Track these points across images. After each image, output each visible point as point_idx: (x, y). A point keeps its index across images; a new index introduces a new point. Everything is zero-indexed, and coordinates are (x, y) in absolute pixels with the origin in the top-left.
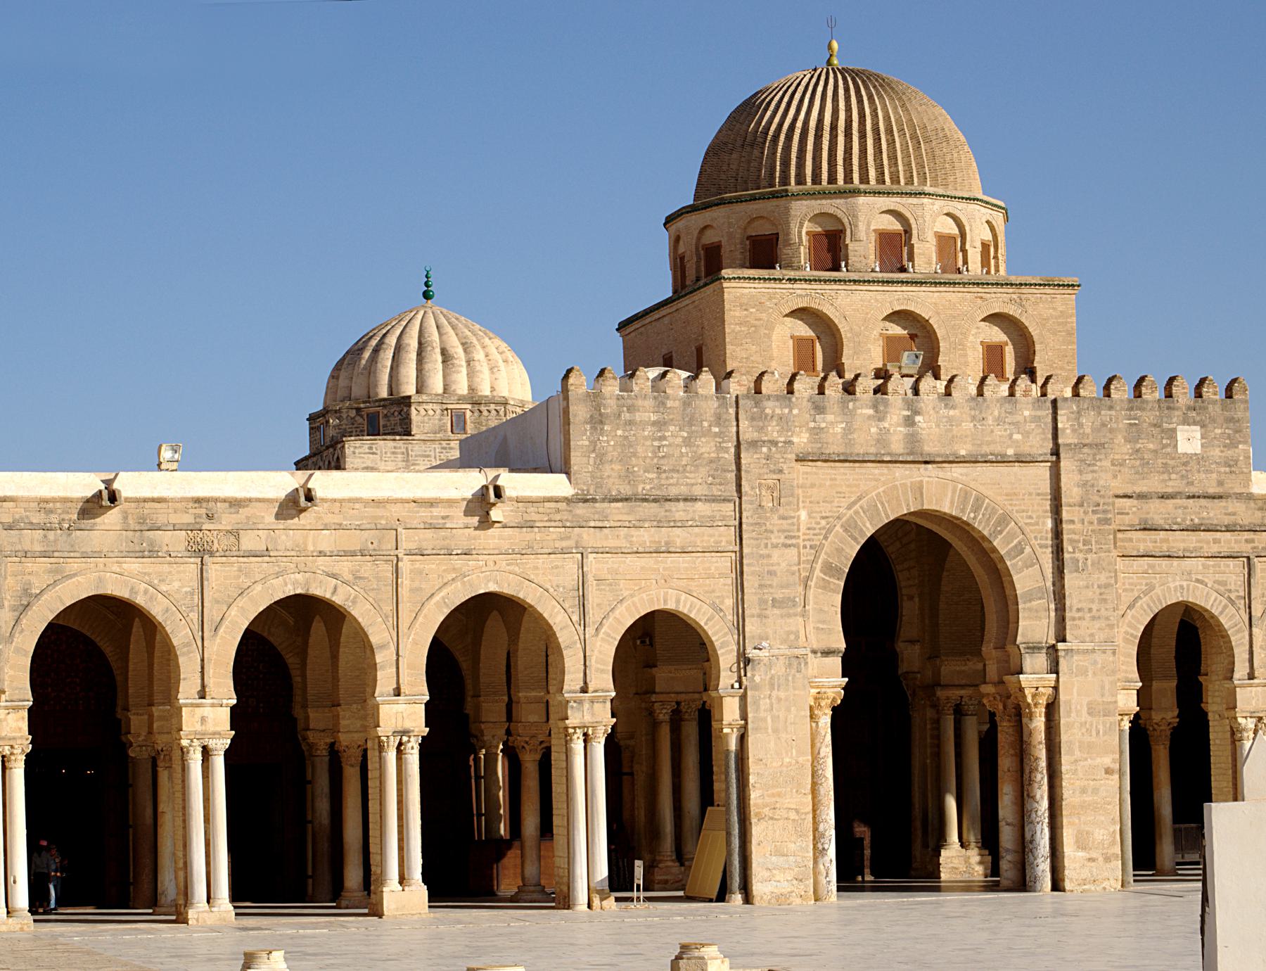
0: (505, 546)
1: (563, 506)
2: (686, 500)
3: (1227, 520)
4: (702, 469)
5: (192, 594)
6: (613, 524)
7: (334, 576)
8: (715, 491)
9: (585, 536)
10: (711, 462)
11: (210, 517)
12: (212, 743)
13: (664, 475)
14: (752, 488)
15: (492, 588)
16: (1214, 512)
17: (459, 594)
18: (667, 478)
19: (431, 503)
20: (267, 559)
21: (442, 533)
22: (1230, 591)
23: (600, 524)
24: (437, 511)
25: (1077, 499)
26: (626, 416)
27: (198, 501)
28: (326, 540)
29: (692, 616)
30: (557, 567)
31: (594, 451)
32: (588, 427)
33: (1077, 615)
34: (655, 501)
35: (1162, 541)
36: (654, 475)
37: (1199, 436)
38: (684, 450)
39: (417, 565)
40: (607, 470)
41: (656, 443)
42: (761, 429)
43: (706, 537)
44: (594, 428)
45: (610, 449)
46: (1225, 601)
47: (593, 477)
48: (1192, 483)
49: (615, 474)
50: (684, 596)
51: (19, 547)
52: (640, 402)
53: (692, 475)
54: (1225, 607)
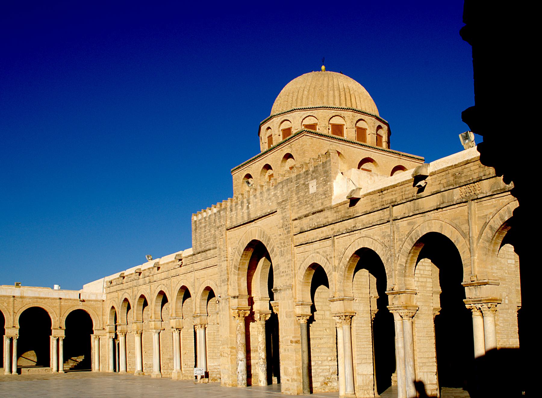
3: (324, 221)
7: (164, 285)
16: (320, 219)
22: (327, 255)
25: (281, 226)
28: (164, 275)
33: (282, 275)
35: (308, 236)
37: (315, 183)
42: (220, 222)
46: (326, 260)
48: (313, 207)
54: (326, 263)
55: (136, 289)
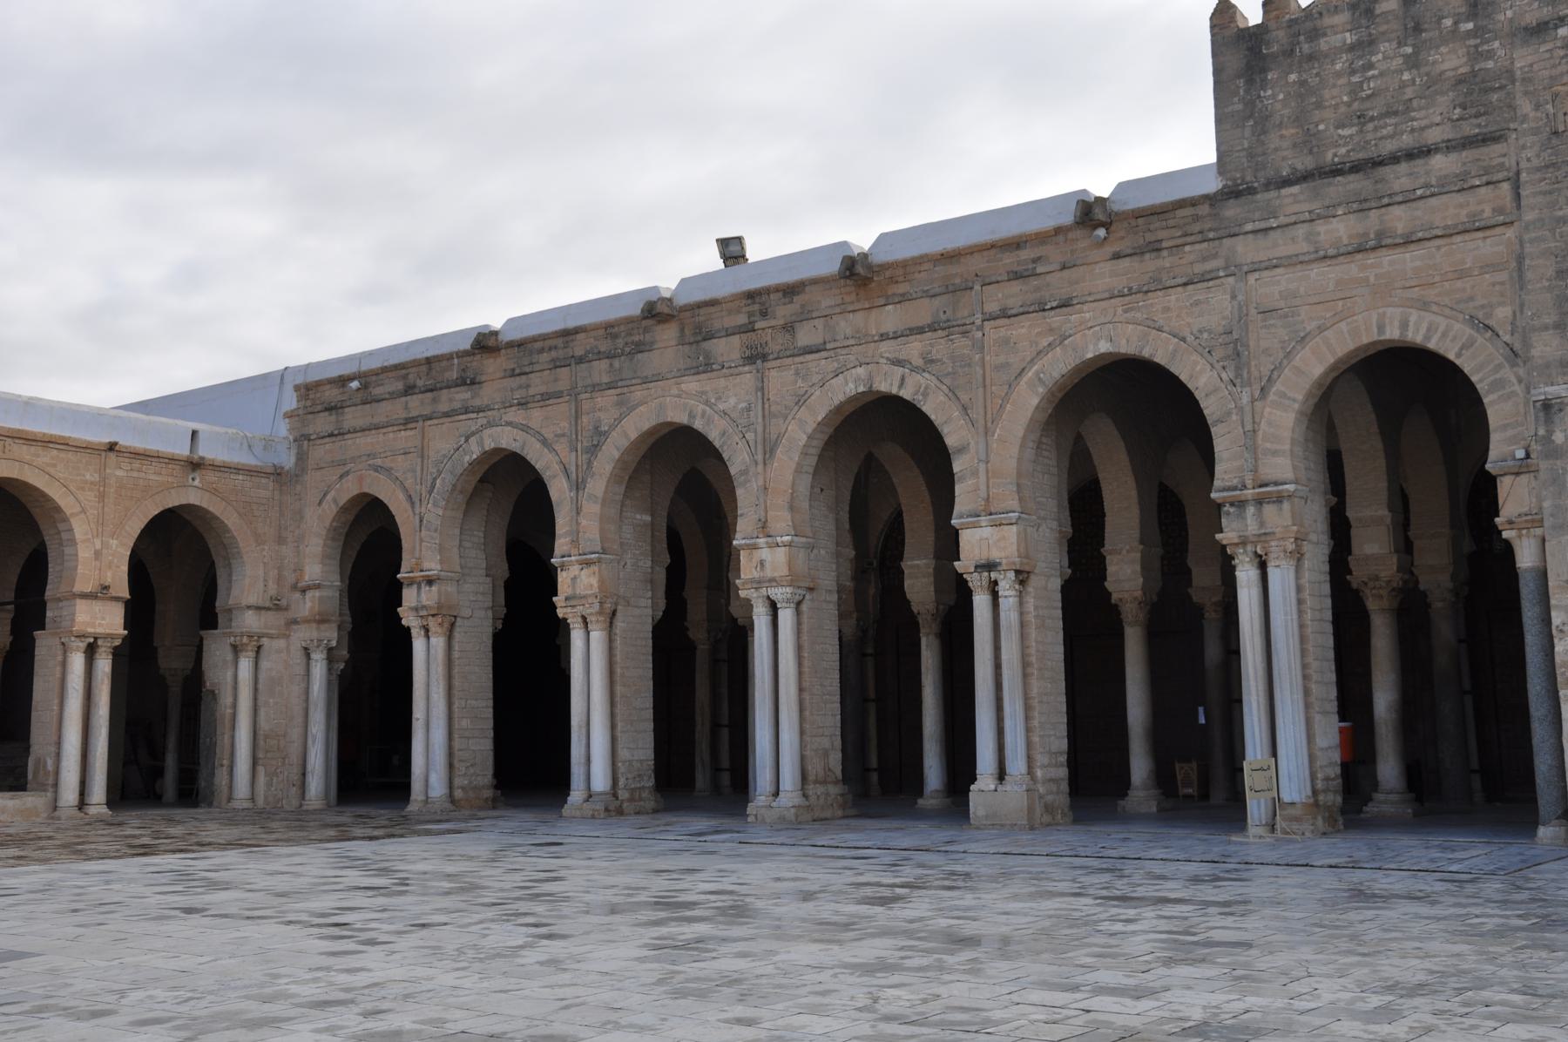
0: (1119, 283)
1: (1204, 209)
2: (1410, 155)
4: (1441, 99)
5: (749, 409)
6: (1283, 220)
7: (898, 363)
8: (1469, 129)
9: (1240, 249)
10: (1460, 81)
11: (764, 314)
12: (778, 593)
13: (1370, 126)
14: (1537, 107)
15: (1104, 347)
17: (1059, 365)
18: (1376, 129)
19: (1015, 244)
20: (824, 354)
21: (1034, 282)
23: (1263, 225)
24: (1026, 254)
26: (1306, 47)
27: (751, 295)
29: (1432, 345)
30: (1197, 303)
31: (1251, 116)
32: (1241, 82)
34: (1356, 168)
36: (1354, 130)
38: (1406, 76)
39: (1003, 332)
40: (1273, 141)
41: (1356, 79)
43: (1449, 210)
44: (1250, 82)
45: (1278, 106)
47: (1251, 156)
49: (1285, 144)
50: (1414, 316)
51: (589, 382)
52: (1328, 21)
53: (1423, 113)
55: (606, 399)
